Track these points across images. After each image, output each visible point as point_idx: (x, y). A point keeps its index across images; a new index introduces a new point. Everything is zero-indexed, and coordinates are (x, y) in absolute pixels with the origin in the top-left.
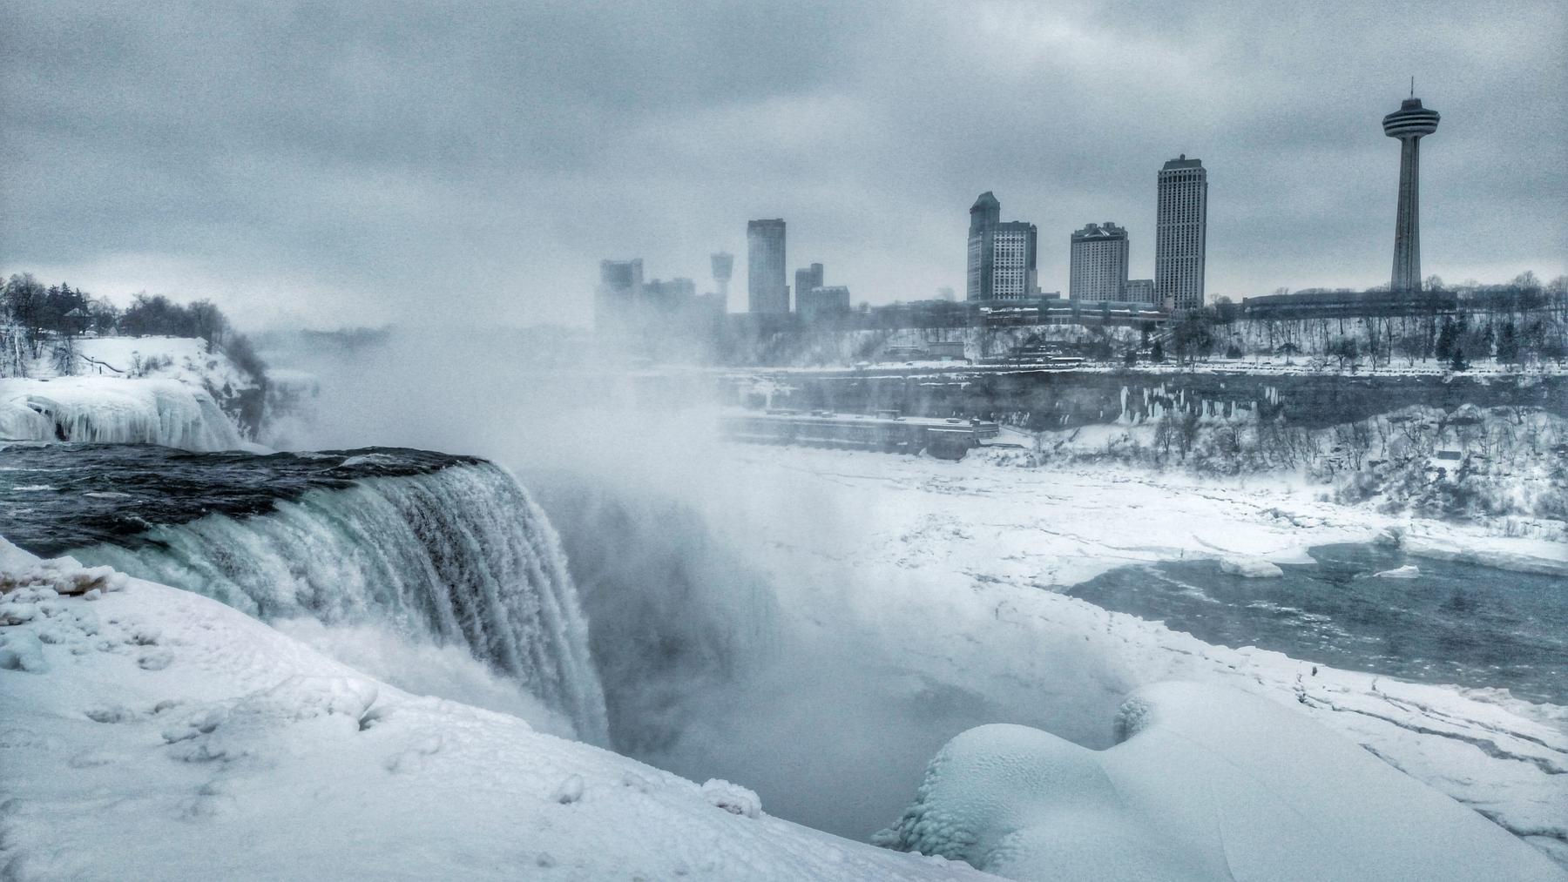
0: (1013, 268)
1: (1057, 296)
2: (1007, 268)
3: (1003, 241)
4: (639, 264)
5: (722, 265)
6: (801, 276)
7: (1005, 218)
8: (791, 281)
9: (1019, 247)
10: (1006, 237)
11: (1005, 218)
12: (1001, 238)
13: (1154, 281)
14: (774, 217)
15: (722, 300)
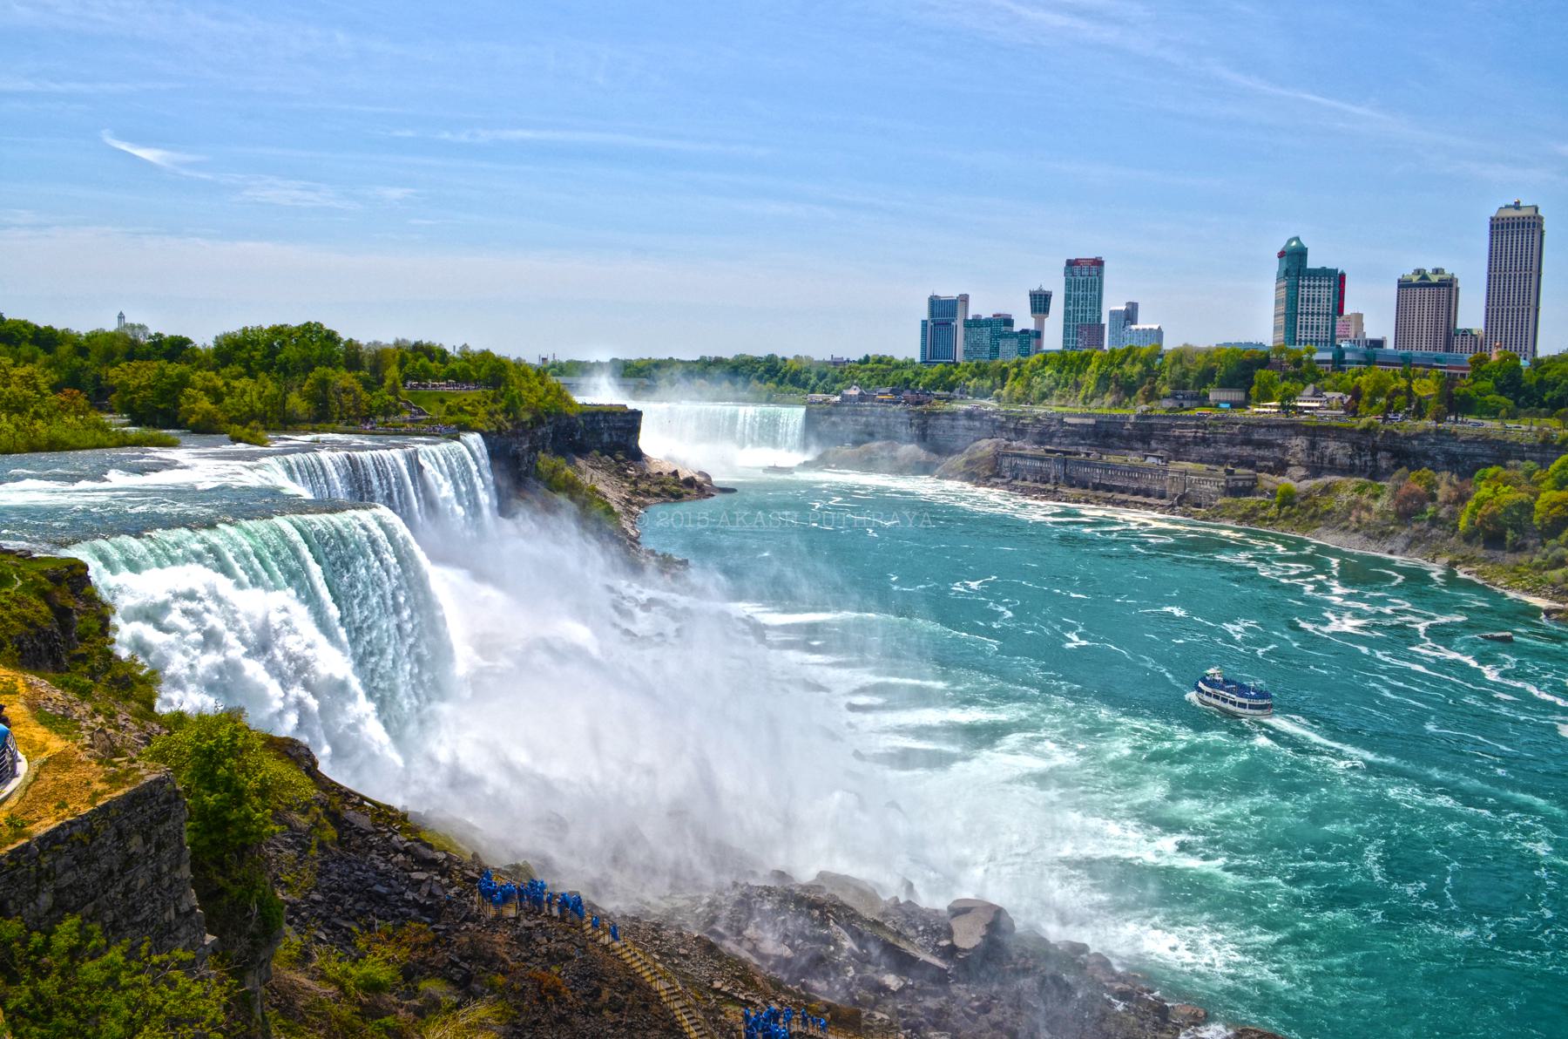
0: (1318, 314)
1: (1379, 343)
2: (1313, 314)
3: (1309, 286)
4: (965, 299)
5: (1040, 302)
6: (1113, 313)
7: (1313, 263)
8: (1105, 320)
9: (1326, 293)
10: (1312, 283)
11: (1313, 263)
12: (1306, 283)
13: (1483, 334)
14: (1092, 256)
15: (1038, 334)
